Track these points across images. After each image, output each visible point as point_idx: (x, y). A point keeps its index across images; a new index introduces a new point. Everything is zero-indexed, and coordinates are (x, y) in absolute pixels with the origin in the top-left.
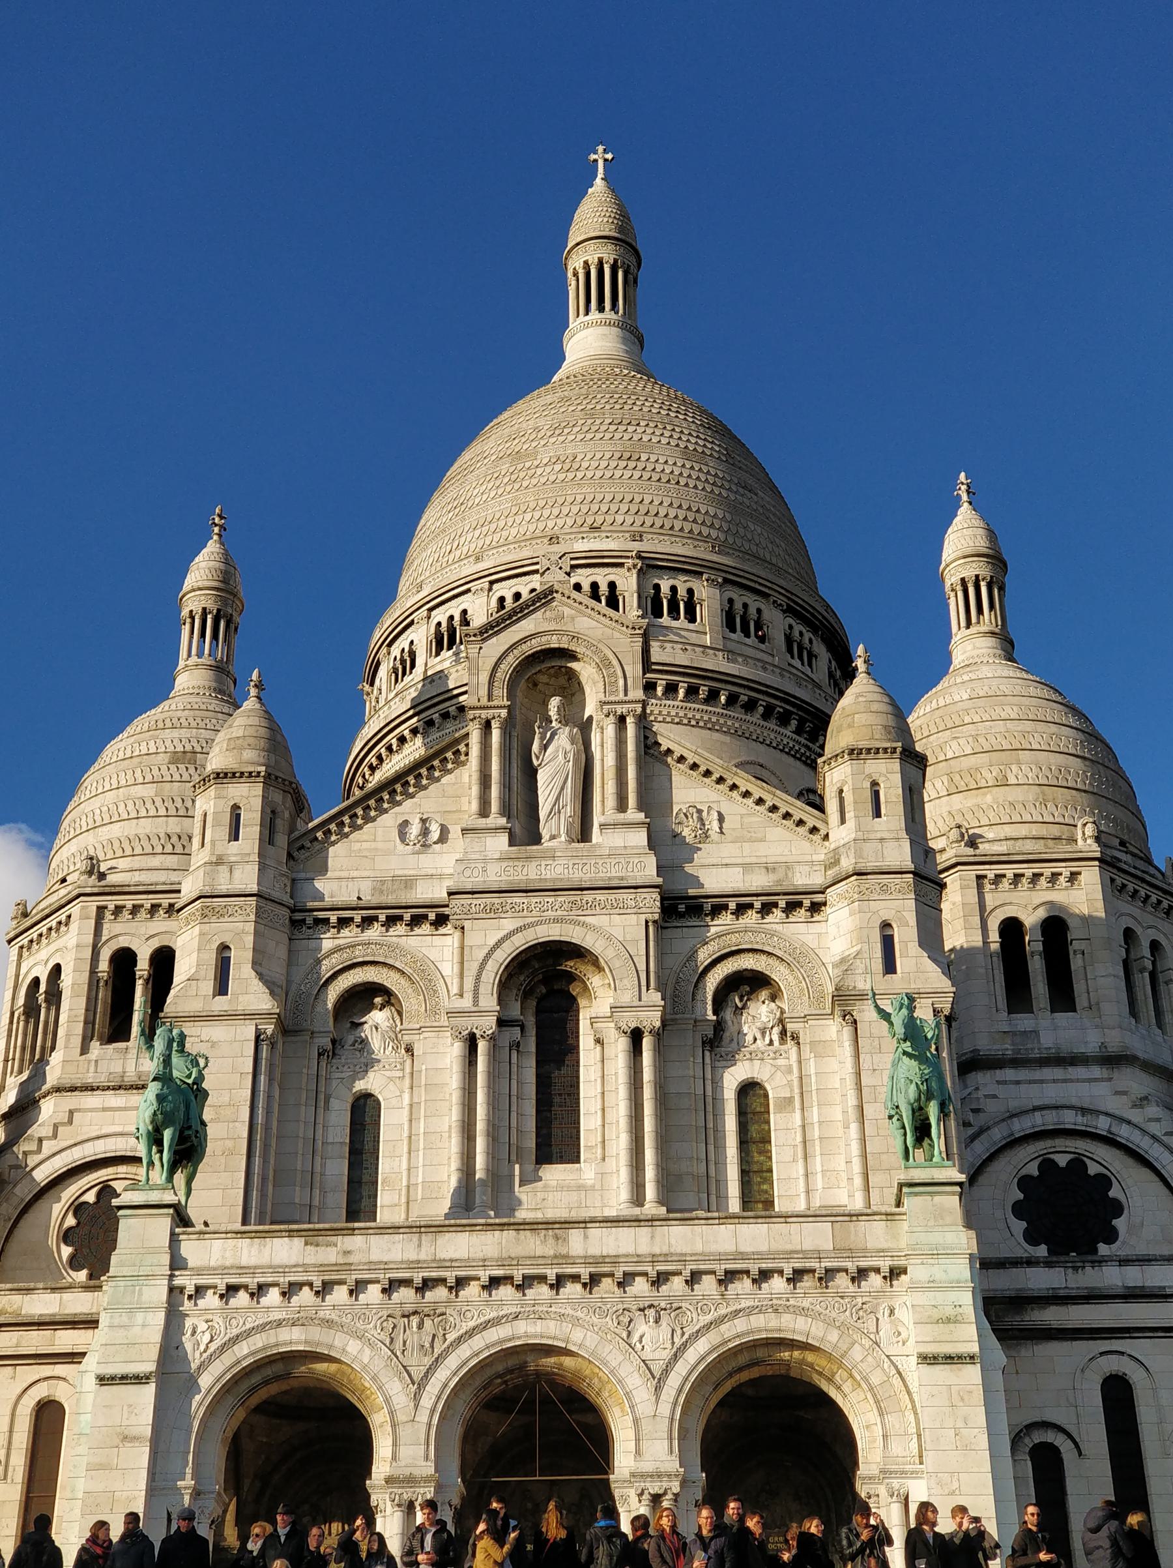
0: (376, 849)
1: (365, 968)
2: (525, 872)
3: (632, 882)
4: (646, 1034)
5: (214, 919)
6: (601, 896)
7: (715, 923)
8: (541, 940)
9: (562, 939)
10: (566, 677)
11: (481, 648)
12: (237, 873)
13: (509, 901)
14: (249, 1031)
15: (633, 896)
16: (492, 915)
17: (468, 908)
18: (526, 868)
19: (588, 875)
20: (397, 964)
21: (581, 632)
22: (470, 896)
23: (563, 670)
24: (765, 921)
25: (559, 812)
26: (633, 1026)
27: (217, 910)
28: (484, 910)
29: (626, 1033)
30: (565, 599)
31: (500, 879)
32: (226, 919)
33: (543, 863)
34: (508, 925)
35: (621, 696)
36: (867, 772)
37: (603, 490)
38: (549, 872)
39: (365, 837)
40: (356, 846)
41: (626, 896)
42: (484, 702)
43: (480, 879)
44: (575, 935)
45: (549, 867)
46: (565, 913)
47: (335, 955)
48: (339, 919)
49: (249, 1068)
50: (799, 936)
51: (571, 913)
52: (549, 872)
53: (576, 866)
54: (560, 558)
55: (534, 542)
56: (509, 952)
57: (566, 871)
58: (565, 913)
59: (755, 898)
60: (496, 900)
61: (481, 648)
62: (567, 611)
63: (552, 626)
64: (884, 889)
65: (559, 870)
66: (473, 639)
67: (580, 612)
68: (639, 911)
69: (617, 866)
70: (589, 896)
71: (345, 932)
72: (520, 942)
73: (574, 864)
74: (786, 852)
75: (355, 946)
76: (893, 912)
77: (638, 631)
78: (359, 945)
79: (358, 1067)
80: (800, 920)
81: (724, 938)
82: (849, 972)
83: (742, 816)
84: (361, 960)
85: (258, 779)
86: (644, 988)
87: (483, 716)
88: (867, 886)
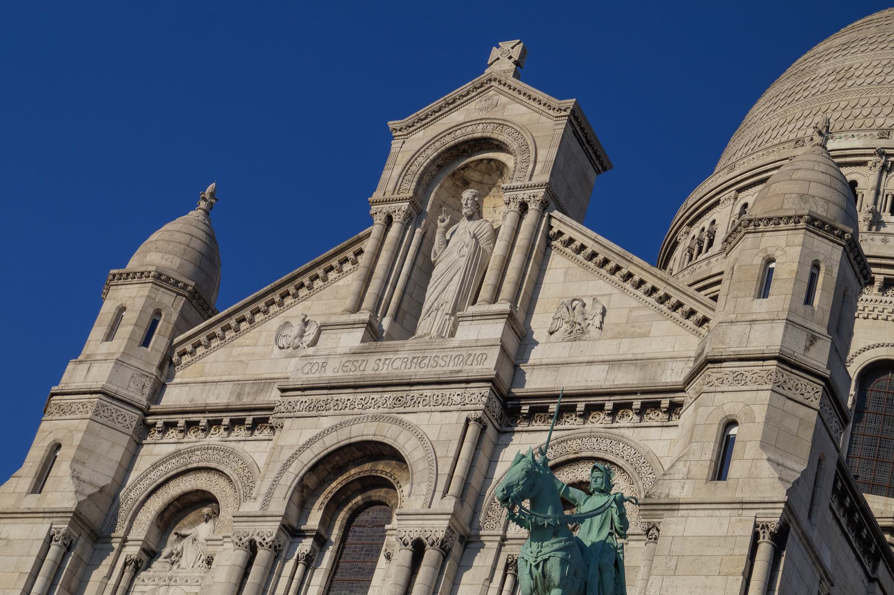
0: (253, 354)
1: (211, 475)
2: (362, 368)
3: (463, 376)
4: (428, 546)
5: (57, 417)
6: (428, 391)
7: (559, 427)
8: (353, 440)
9: (375, 438)
10: (498, 173)
11: (404, 143)
12: (94, 371)
13: (336, 397)
14: (41, 529)
15: (459, 392)
16: (314, 413)
17: (294, 405)
18: (364, 363)
19: (423, 370)
20: (227, 471)
21: (509, 118)
22: (299, 393)
23: (493, 163)
24: (615, 425)
25: (437, 310)
26: (415, 536)
27: (62, 407)
28: (309, 408)
29: (406, 545)
30: (501, 87)
31: (337, 374)
32: (68, 417)
33: (383, 357)
34: (326, 423)
35: (527, 182)
36: (762, 246)
37: (869, 95)
38: (386, 367)
39: (248, 342)
40: (236, 351)
41: (454, 393)
42: (388, 196)
43: (317, 375)
44: (389, 434)
45: (387, 362)
46: (386, 410)
47: (174, 461)
48: (187, 422)
49: (28, 567)
50: (646, 442)
51: (396, 410)
52: (386, 367)
53: (415, 361)
54: (513, 48)
55: (781, 147)
56: (316, 452)
57: (404, 365)
58: (386, 410)
59: (607, 398)
60: (320, 397)
61: (404, 143)
62: (503, 99)
63: (484, 115)
64: (738, 378)
65: (397, 364)
66: (400, 133)
67: (514, 99)
68: (463, 408)
69: (457, 359)
70: (415, 392)
71: (191, 436)
72: (332, 442)
73: (414, 358)
74: (669, 349)
75: (194, 451)
76: (741, 406)
77: (563, 113)
78: (198, 450)
79: (162, 580)
80: (655, 424)
81: (564, 444)
82: (667, 477)
83: (631, 309)
84: (195, 465)
85: (148, 280)
86: (438, 494)
87: (384, 211)
88: (719, 375)
